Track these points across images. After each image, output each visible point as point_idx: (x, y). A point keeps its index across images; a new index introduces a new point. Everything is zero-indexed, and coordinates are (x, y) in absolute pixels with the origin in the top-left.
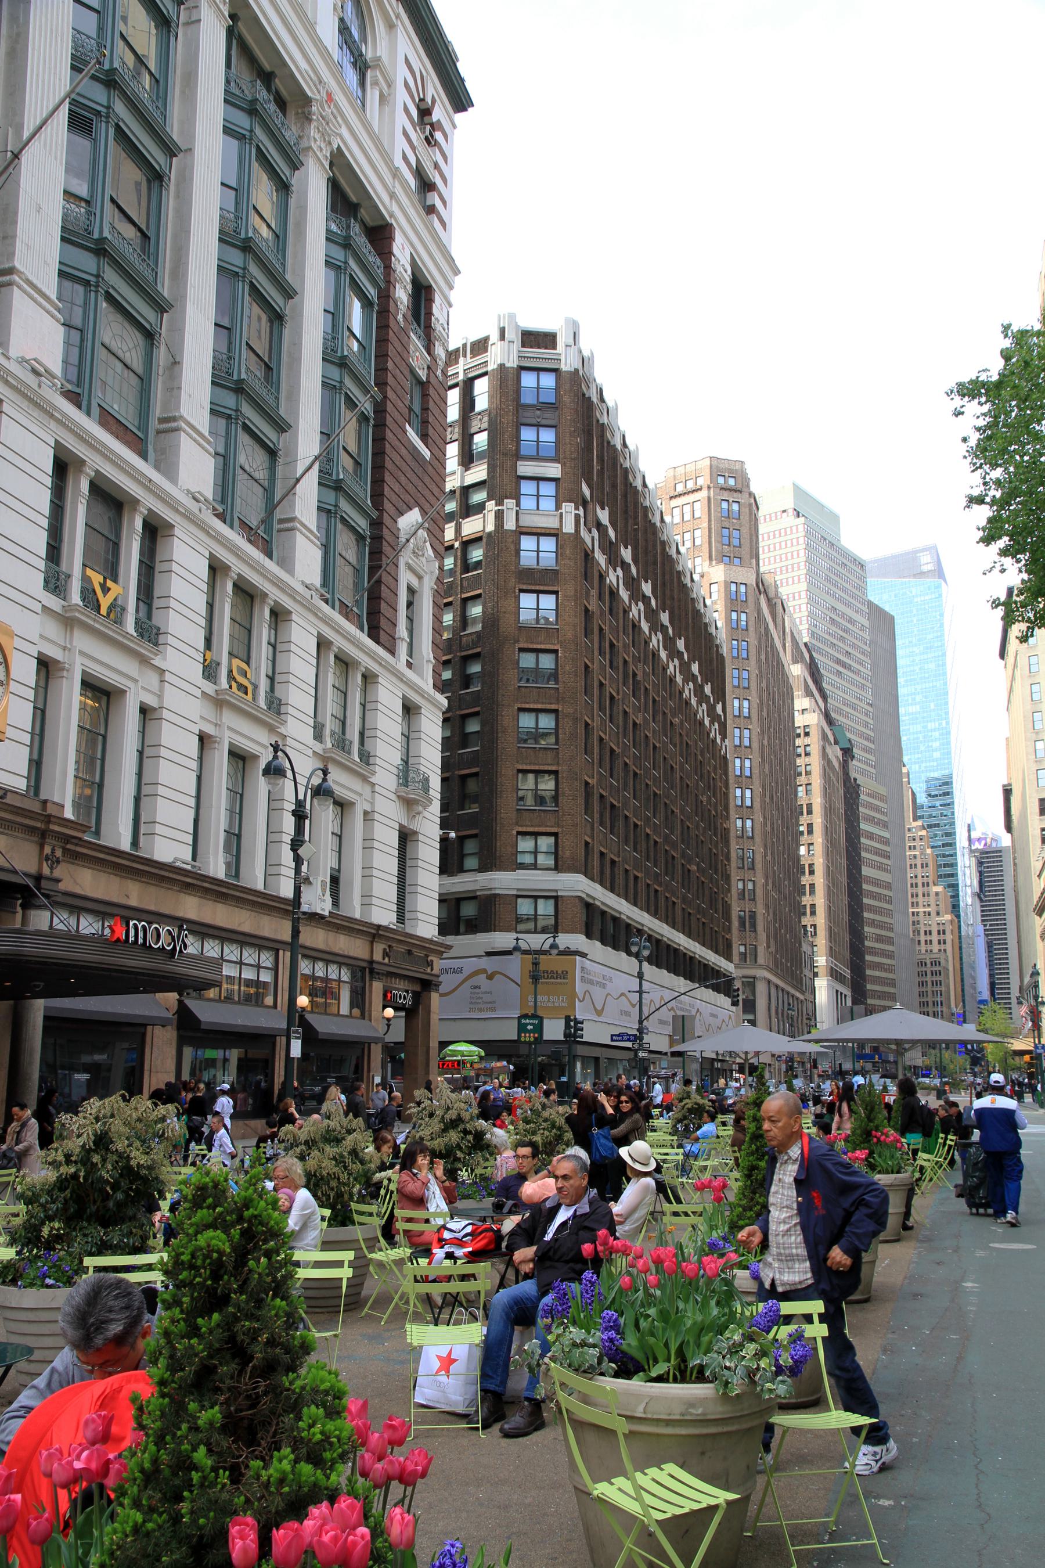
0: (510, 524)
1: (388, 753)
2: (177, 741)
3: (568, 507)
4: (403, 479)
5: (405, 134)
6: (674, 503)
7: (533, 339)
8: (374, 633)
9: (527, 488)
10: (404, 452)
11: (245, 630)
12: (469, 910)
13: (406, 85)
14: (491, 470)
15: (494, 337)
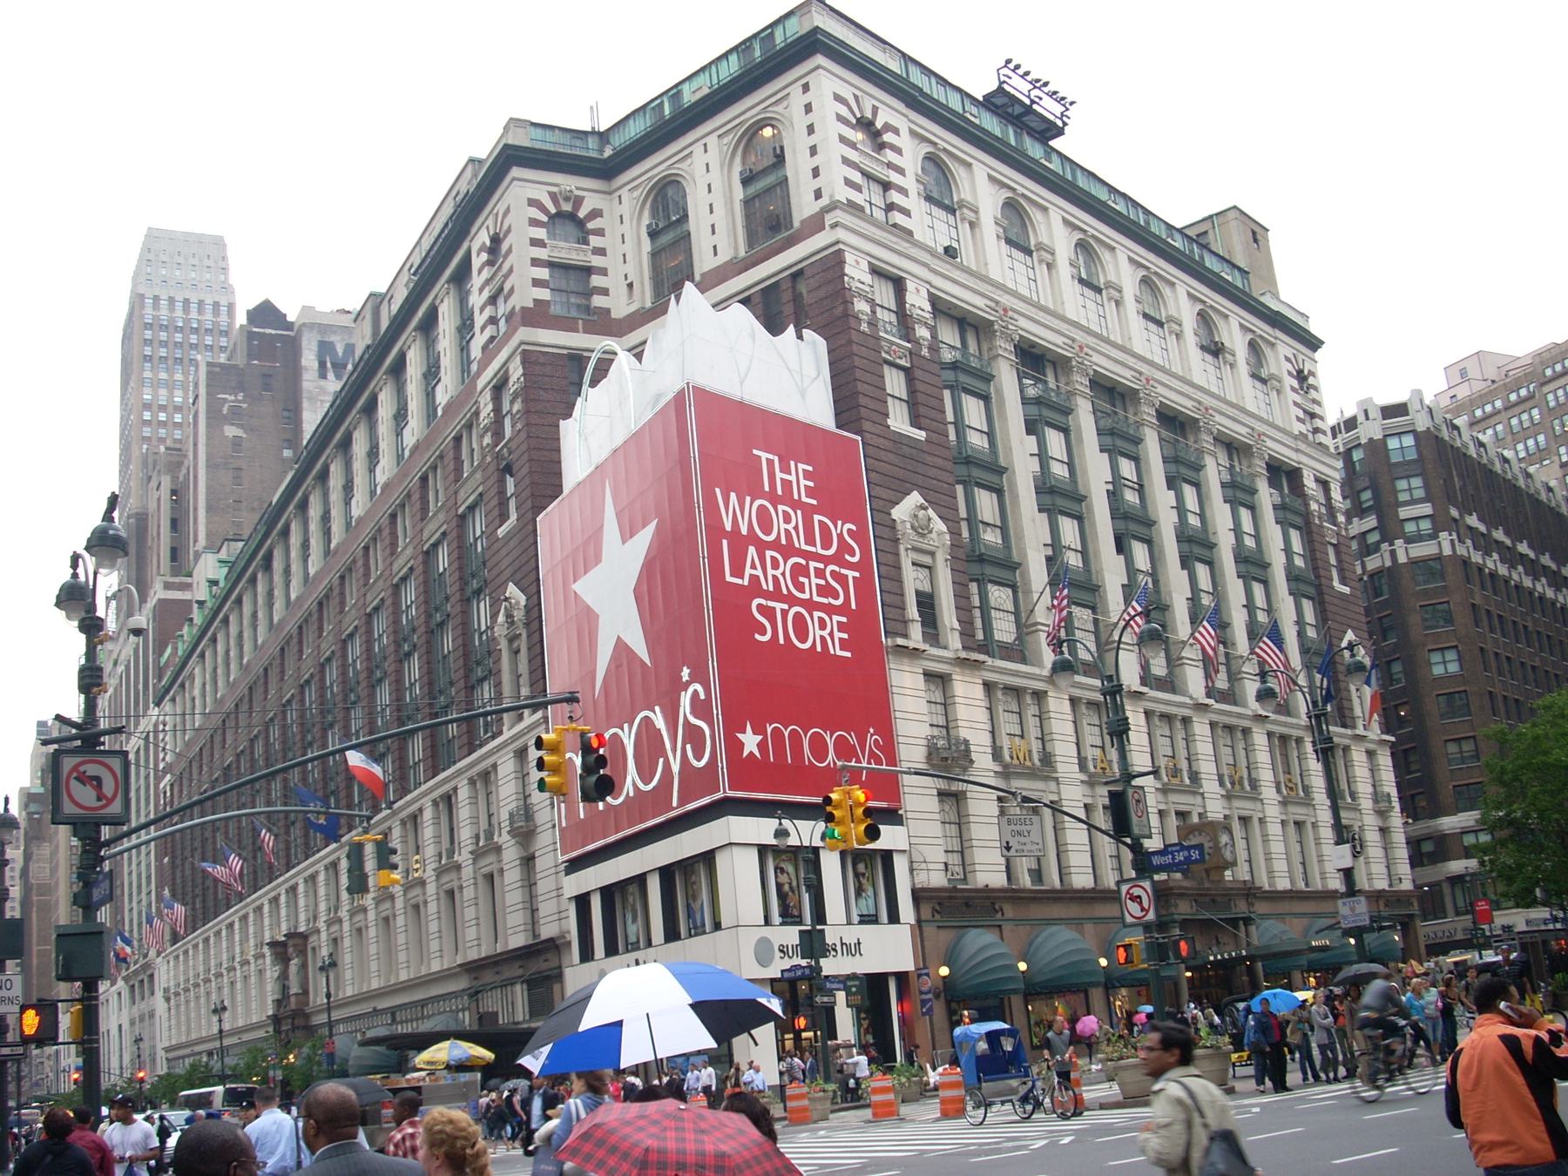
0: (1402, 559)
1: (1364, 788)
2: (1274, 829)
3: (1443, 535)
4: (1339, 618)
5: (1296, 404)
6: (1546, 389)
7: (1390, 411)
8: (1344, 726)
9: (1410, 528)
10: (1336, 601)
11: (1285, 756)
12: (1427, 847)
13: (1290, 373)
14: (1380, 519)
15: (1361, 418)
